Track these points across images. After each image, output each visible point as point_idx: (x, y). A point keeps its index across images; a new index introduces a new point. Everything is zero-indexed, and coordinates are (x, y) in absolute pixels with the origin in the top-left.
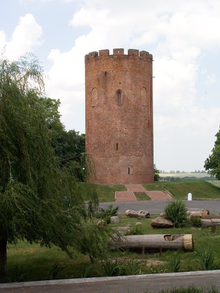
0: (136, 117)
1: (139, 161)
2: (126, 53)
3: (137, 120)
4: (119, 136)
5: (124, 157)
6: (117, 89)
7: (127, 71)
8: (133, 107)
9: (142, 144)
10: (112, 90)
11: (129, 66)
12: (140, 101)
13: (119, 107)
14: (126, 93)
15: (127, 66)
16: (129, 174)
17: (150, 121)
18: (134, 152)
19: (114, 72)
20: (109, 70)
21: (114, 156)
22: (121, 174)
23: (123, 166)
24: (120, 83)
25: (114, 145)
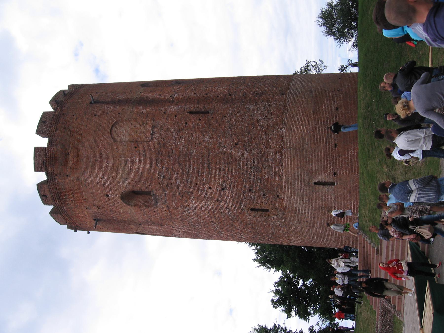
3: (186, 155)
4: (230, 205)
5: (285, 196)
6: (121, 202)
7: (78, 179)
9: (250, 141)
10: (127, 213)
12: (141, 146)
14: (126, 184)
16: (333, 184)
17: (192, 107)
19: (87, 207)
20: (86, 213)
21: (285, 218)
25: (255, 217)
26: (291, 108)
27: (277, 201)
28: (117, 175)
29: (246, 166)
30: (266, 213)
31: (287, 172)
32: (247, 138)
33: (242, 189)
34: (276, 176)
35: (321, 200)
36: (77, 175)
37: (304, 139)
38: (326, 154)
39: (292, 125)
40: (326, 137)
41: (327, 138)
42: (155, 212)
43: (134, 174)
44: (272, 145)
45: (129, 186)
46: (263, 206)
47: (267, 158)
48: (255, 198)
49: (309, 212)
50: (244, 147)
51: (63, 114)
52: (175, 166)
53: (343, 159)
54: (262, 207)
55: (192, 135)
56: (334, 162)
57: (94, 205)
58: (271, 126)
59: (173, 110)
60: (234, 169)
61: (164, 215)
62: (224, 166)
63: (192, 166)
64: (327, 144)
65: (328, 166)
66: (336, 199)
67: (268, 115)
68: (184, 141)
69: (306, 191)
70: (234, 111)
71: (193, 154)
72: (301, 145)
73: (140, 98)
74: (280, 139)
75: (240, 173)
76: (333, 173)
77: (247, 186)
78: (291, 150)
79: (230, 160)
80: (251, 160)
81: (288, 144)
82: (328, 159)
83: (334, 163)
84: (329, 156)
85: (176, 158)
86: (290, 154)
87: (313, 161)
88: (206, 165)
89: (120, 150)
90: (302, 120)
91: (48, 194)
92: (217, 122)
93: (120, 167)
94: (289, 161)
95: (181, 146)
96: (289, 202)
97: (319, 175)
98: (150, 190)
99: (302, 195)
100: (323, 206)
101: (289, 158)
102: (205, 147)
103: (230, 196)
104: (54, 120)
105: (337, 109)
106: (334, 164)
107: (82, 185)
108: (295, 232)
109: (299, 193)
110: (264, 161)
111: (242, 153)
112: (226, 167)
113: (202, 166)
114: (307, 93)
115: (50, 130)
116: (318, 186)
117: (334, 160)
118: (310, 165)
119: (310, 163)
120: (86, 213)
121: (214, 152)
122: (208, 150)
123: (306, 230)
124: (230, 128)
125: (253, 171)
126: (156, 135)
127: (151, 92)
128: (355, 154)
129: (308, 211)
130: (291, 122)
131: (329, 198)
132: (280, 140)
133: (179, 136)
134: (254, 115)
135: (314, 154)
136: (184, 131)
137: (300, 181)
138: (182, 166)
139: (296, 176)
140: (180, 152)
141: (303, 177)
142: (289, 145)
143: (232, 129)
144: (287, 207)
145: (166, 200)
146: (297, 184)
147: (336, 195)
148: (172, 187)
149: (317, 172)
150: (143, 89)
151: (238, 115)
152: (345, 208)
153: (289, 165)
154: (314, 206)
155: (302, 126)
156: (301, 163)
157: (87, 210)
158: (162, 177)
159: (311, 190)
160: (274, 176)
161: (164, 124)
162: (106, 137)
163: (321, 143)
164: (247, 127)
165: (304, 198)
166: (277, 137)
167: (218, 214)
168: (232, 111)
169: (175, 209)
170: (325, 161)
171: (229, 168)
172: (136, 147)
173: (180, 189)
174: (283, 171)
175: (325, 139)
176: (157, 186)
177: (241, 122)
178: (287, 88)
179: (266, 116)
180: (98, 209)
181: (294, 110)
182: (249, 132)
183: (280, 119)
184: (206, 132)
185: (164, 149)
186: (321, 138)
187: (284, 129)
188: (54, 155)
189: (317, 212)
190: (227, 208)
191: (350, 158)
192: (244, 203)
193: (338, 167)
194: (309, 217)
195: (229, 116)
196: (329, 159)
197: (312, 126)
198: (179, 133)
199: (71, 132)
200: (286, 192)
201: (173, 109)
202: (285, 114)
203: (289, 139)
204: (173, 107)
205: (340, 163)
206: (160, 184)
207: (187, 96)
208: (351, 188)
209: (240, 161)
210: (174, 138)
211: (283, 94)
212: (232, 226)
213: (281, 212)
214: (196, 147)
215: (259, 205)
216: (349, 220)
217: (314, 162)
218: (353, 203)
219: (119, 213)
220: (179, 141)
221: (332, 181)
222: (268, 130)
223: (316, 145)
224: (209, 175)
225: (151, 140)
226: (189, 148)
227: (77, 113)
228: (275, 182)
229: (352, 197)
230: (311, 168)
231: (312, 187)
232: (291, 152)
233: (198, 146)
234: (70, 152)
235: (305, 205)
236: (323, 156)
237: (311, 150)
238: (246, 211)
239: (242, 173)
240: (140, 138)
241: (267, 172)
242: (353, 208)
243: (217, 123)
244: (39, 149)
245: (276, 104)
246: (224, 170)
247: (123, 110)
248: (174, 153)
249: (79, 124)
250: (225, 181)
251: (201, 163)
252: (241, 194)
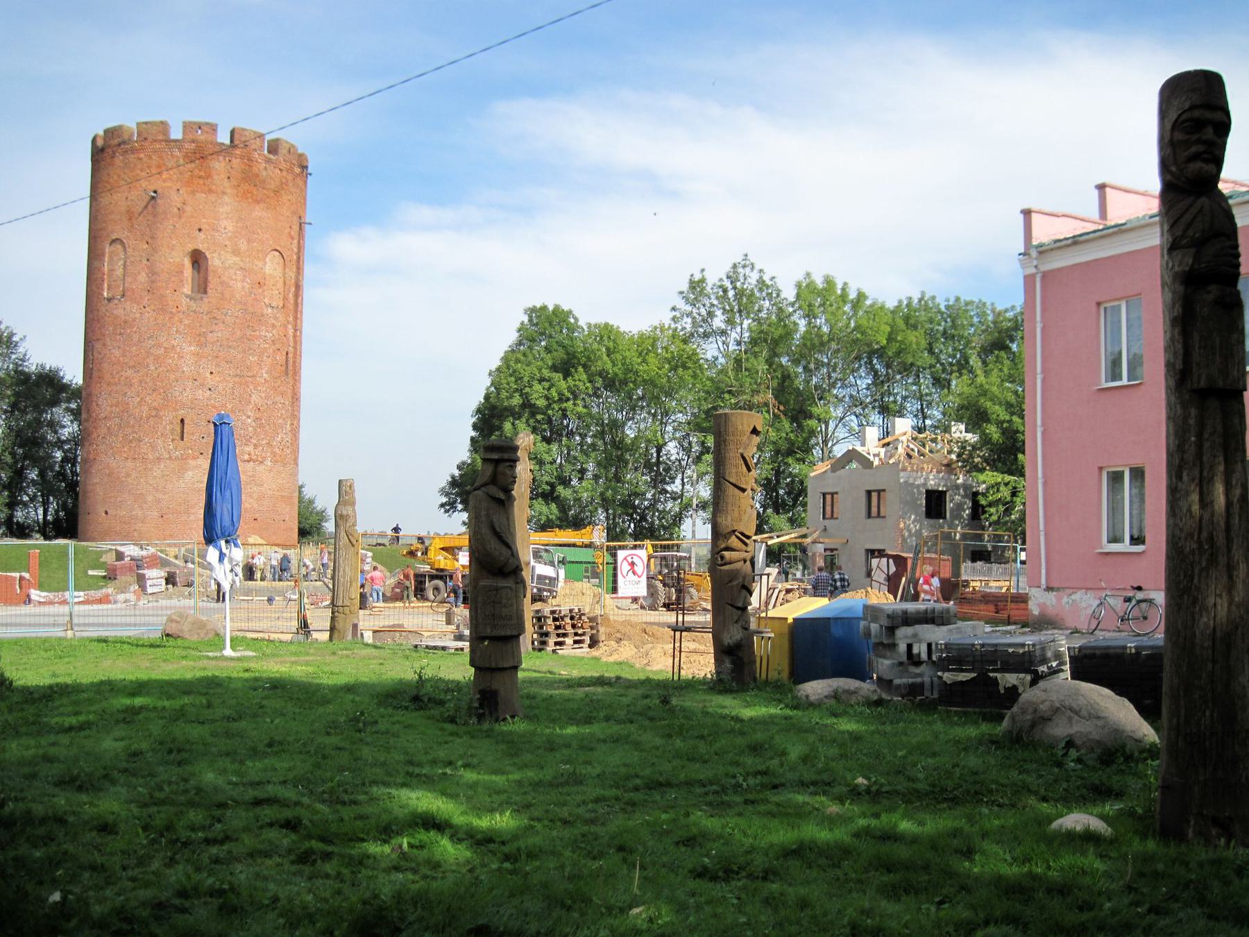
2: (224, 138)
3: (249, 348)
6: (190, 247)
7: (224, 193)
8: (239, 306)
9: (261, 426)
12: (260, 290)
13: (193, 305)
15: (226, 180)
17: (290, 355)
21: (170, 458)
24: (200, 230)
30: (178, 438)
55: (268, 357)
98: (209, 294)
108: (145, 469)
123: (151, 482)
126: (270, 310)
157: (174, 188)
169: (181, 322)
201: (291, 332)
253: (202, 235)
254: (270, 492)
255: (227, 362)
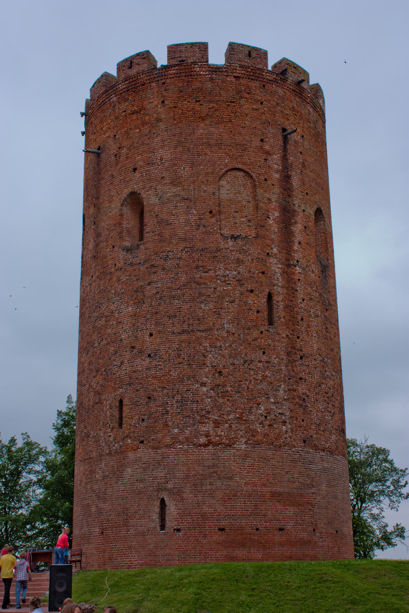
0: (193, 285)
1: (209, 467)
3: (200, 293)
4: (126, 367)
5: (140, 453)
6: (127, 191)
7: (159, 120)
8: (182, 245)
9: (225, 395)
10: (111, 202)
11: (166, 102)
12: (214, 220)
14: (154, 200)
16: (163, 527)
18: (187, 432)
20: (107, 135)
21: (110, 454)
22: (132, 531)
23: (139, 493)
24: (135, 170)
26: (280, 455)
27: (134, 441)
28: (166, 184)
29: (186, 391)
30: (116, 425)
31: (179, 455)
32: (229, 389)
33: (151, 385)
34: (172, 438)
35: (138, 510)
36: (165, 118)
37: (230, 480)
38: (207, 515)
39: (252, 460)
40: (234, 513)
41: (233, 515)
42: (113, 247)
43: (170, 213)
44: (220, 429)
45: (150, 205)
46: (127, 419)
47: (200, 423)
48: (138, 406)
49: (120, 491)
50: (216, 385)
51: (264, 86)
52: (184, 278)
53: (201, 541)
54: (126, 417)
56: (196, 527)
57: (120, 148)
58: (251, 427)
59: (273, 268)
60: (181, 372)
61: (110, 263)
62: (186, 356)
63: (185, 305)
64: (223, 515)
65: (190, 518)
66: (140, 533)
67: (268, 420)
68: (223, 290)
69: (150, 486)
70: (273, 366)
71: (203, 306)
72: (221, 475)
73: (294, 211)
74: (230, 441)
75: (174, 381)
76: (179, 527)
77: (155, 394)
78: (213, 459)
79: (194, 365)
80: (195, 397)
81: (221, 454)
82: (200, 518)
83: (194, 528)
84: (205, 520)
85: (195, 278)
86: (205, 459)
87: (197, 494)
88: (185, 327)
89: (206, 187)
90: (261, 474)
91: (134, 71)
92: (256, 339)
93: (179, 188)
94: (196, 457)
95: (214, 285)
96: (133, 460)
97: (176, 505)
98: (145, 240)
99: (144, 480)
100: (129, 513)
101: (199, 457)
102: (213, 324)
103: (140, 367)
104: (253, 71)
105: (281, 529)
106: (193, 527)
107: (149, 127)
109: (147, 475)
110: (194, 418)
111: (206, 383)
112: (184, 359)
113: (185, 321)
114: (307, 481)
115: (237, 66)
116: (159, 503)
117: (199, 527)
118: (190, 490)
119: (193, 490)
120: (107, 135)
121: (206, 338)
122: (209, 329)
123: (95, 487)
124: (245, 362)
125: (179, 402)
126: (230, 243)
127: (305, 227)
128: (209, 560)
129: (122, 491)
130: (257, 458)
131: (141, 521)
132: (228, 442)
133: (231, 281)
134: (268, 398)
135: (207, 497)
136: (239, 288)
137: (166, 476)
138: (184, 289)
139: (172, 469)
140: (205, 284)
141: (172, 481)
142: (221, 456)
143: (243, 365)
144: (126, 456)
145: (131, 266)
146: (160, 472)
147: (146, 533)
148: (150, 274)
149: (180, 502)
150: (311, 214)
151: (267, 372)
152: (127, 547)
153: (189, 457)
154: (129, 499)
155: (252, 476)
156: (192, 475)
158: (165, 258)
159: (153, 493)
160: (172, 435)
161: (249, 255)
162: (226, 161)
163: (225, 506)
164: (248, 388)
165: (140, 482)
166: (233, 436)
167: (113, 348)
168: (274, 363)
169: (119, 280)
170: (197, 513)
171: (181, 363)
172: (211, 212)
173: (148, 287)
174: (180, 448)
175: (231, 513)
176: (152, 250)
177: (254, 378)
178: (316, 448)
179: (266, 417)
180: (115, 154)
181: (278, 462)
182: (239, 392)
183: (262, 440)
184: (238, 323)
185: (209, 259)
186: (233, 506)
187: (245, 448)
188: (196, 76)
189: (120, 504)
190: (122, 363)
191: (201, 553)
192: (130, 390)
193: (188, 535)
194: (113, 491)
195: (264, 358)
196: (200, 520)
197: (251, 491)
198: (235, 280)
199: (234, 102)
200: (148, 454)
202: (270, 448)
203: (230, 456)
204: (278, 268)
205: (194, 537)
206: (155, 255)
207: (298, 288)
208: (157, 556)
209: (194, 380)
210: (227, 272)
211: (304, 442)
212: (97, 371)
213: (118, 448)
214: (214, 310)
215: (128, 413)
216: (110, 555)
217: (195, 497)
218: (134, 561)
219: (110, 190)
220: (223, 282)
221: (167, 526)
222: (243, 422)
223: (221, 498)
224: (170, 332)
225: (223, 237)
226: (212, 298)
227: (266, 109)
228: (163, 437)
229: (144, 558)
230: (186, 492)
231: (156, 495)
232: (209, 459)
233: (215, 312)
234: (201, 105)
235: (130, 486)
236: (204, 511)
237: (213, 492)
238: (118, 393)
239: (175, 385)
240: (225, 219)
241: (178, 424)
242: (127, 561)
243: (253, 340)
244: (204, 51)
245: (287, 432)
246: (179, 355)
247: (273, 185)
248: (203, 274)
249: (247, 115)
250: (163, 358)
251: (189, 319)
252: (142, 384)
253: (138, 175)
254: (249, 488)
255: (169, 317)
